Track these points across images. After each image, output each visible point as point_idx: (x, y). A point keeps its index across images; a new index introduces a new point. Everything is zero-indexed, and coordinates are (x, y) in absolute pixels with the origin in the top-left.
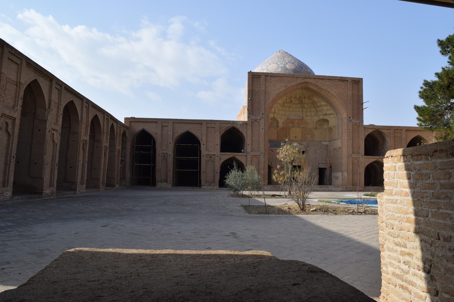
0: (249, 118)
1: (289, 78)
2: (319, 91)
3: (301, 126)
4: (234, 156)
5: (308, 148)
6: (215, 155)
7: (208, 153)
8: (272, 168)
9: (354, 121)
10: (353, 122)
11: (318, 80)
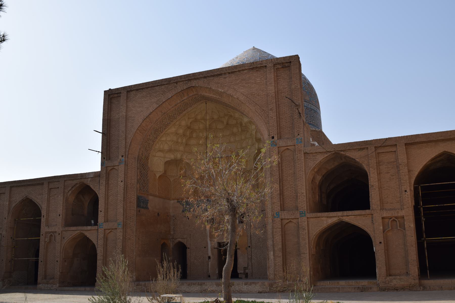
0: (103, 166)
1: (163, 87)
2: (219, 98)
4: (82, 232)
6: (56, 232)
7: (48, 230)
8: (188, 249)
9: (281, 143)
10: (281, 145)
11: (212, 78)
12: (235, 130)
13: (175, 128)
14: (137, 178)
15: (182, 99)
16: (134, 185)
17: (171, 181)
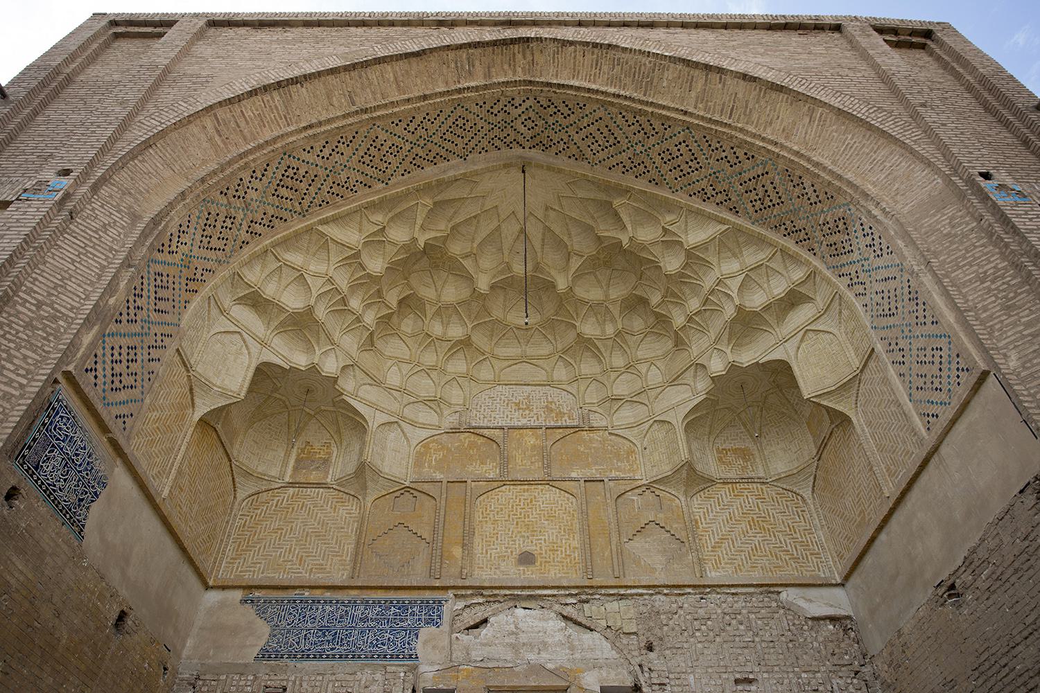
3: (574, 475)
5: (652, 655)
12: (589, 328)
13: (360, 231)
14: (100, 298)
15: (459, 82)
16: (61, 323)
17: (239, 498)
